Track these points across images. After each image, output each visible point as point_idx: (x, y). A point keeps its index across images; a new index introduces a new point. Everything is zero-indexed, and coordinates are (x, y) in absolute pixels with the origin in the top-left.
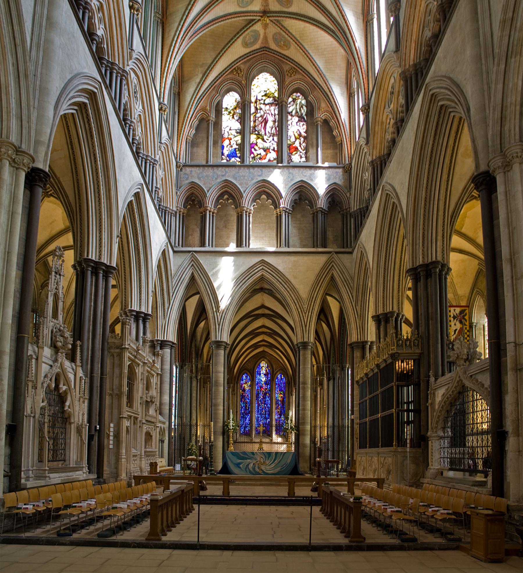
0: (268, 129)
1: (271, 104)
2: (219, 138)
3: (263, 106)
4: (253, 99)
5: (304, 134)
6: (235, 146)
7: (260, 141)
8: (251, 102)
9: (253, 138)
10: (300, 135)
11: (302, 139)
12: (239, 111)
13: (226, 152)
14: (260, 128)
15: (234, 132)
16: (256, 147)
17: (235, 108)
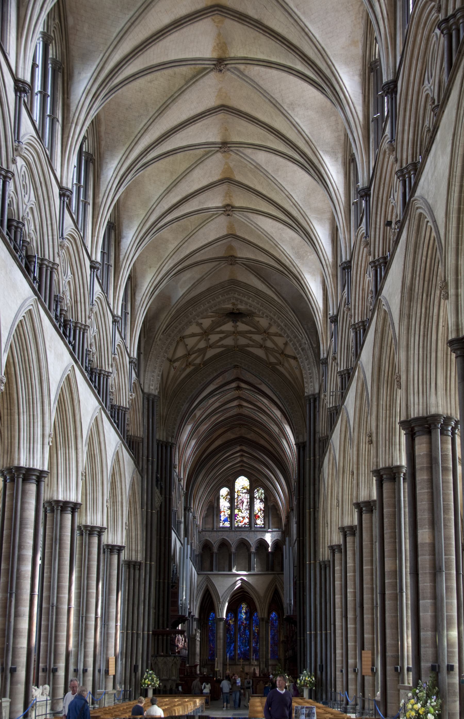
0: (244, 506)
1: (246, 493)
2: (219, 511)
3: (241, 494)
4: (236, 490)
5: (263, 509)
6: (227, 516)
7: (240, 513)
8: (235, 492)
9: (236, 511)
10: (261, 509)
11: (262, 512)
12: (229, 497)
13: (222, 518)
14: (240, 506)
15: (226, 508)
16: (238, 516)
17: (227, 495)
